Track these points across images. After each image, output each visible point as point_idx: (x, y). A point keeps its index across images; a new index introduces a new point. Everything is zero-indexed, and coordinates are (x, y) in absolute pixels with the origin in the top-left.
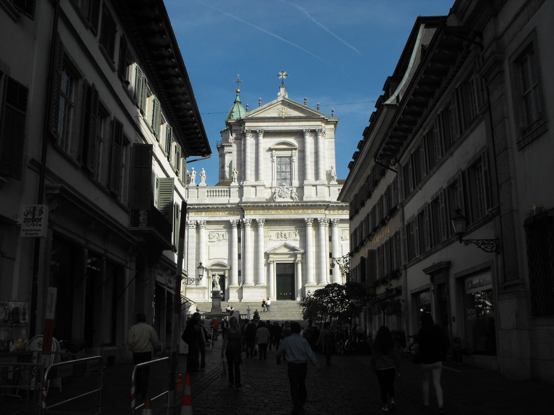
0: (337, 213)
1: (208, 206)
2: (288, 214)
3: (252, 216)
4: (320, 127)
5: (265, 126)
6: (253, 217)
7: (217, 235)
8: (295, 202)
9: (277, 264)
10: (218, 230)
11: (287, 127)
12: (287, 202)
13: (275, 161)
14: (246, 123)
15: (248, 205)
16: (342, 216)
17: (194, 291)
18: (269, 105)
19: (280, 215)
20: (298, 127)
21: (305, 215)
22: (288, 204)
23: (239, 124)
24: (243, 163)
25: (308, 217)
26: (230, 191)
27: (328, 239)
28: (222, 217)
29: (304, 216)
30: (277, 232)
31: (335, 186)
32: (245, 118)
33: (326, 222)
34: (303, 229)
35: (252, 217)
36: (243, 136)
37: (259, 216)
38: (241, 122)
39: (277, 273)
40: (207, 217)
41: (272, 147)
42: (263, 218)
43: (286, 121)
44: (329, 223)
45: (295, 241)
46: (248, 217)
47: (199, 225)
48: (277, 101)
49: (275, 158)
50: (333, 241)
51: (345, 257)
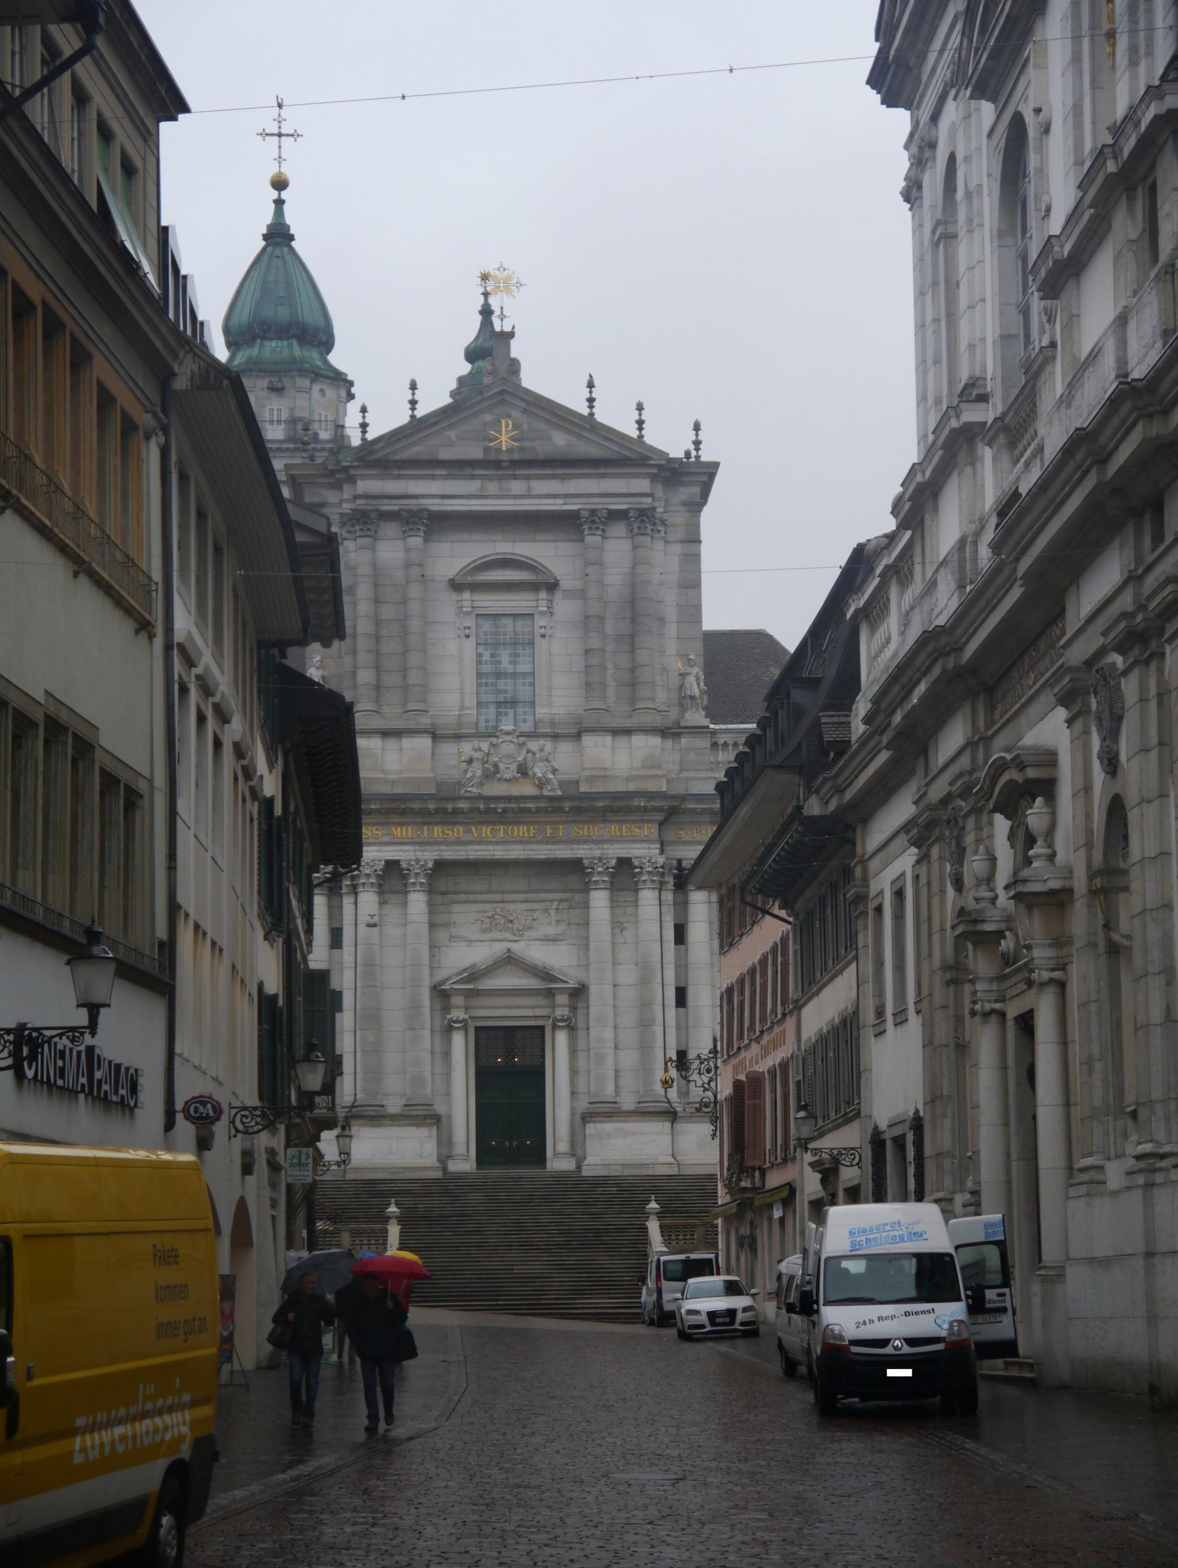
2: (521, 842)
3: (384, 848)
5: (433, 496)
6: (391, 853)
8: (550, 799)
9: (477, 1029)
11: (517, 502)
19: (490, 847)
20: (560, 501)
21: (585, 846)
23: (332, 481)
25: (597, 853)
27: (670, 934)
29: (583, 851)
31: (702, 732)
32: (355, 464)
36: (349, 532)
37: (411, 848)
38: (338, 476)
41: (458, 580)
43: (515, 477)
44: (675, 877)
45: (545, 943)
49: (470, 622)
51: (703, 1057)
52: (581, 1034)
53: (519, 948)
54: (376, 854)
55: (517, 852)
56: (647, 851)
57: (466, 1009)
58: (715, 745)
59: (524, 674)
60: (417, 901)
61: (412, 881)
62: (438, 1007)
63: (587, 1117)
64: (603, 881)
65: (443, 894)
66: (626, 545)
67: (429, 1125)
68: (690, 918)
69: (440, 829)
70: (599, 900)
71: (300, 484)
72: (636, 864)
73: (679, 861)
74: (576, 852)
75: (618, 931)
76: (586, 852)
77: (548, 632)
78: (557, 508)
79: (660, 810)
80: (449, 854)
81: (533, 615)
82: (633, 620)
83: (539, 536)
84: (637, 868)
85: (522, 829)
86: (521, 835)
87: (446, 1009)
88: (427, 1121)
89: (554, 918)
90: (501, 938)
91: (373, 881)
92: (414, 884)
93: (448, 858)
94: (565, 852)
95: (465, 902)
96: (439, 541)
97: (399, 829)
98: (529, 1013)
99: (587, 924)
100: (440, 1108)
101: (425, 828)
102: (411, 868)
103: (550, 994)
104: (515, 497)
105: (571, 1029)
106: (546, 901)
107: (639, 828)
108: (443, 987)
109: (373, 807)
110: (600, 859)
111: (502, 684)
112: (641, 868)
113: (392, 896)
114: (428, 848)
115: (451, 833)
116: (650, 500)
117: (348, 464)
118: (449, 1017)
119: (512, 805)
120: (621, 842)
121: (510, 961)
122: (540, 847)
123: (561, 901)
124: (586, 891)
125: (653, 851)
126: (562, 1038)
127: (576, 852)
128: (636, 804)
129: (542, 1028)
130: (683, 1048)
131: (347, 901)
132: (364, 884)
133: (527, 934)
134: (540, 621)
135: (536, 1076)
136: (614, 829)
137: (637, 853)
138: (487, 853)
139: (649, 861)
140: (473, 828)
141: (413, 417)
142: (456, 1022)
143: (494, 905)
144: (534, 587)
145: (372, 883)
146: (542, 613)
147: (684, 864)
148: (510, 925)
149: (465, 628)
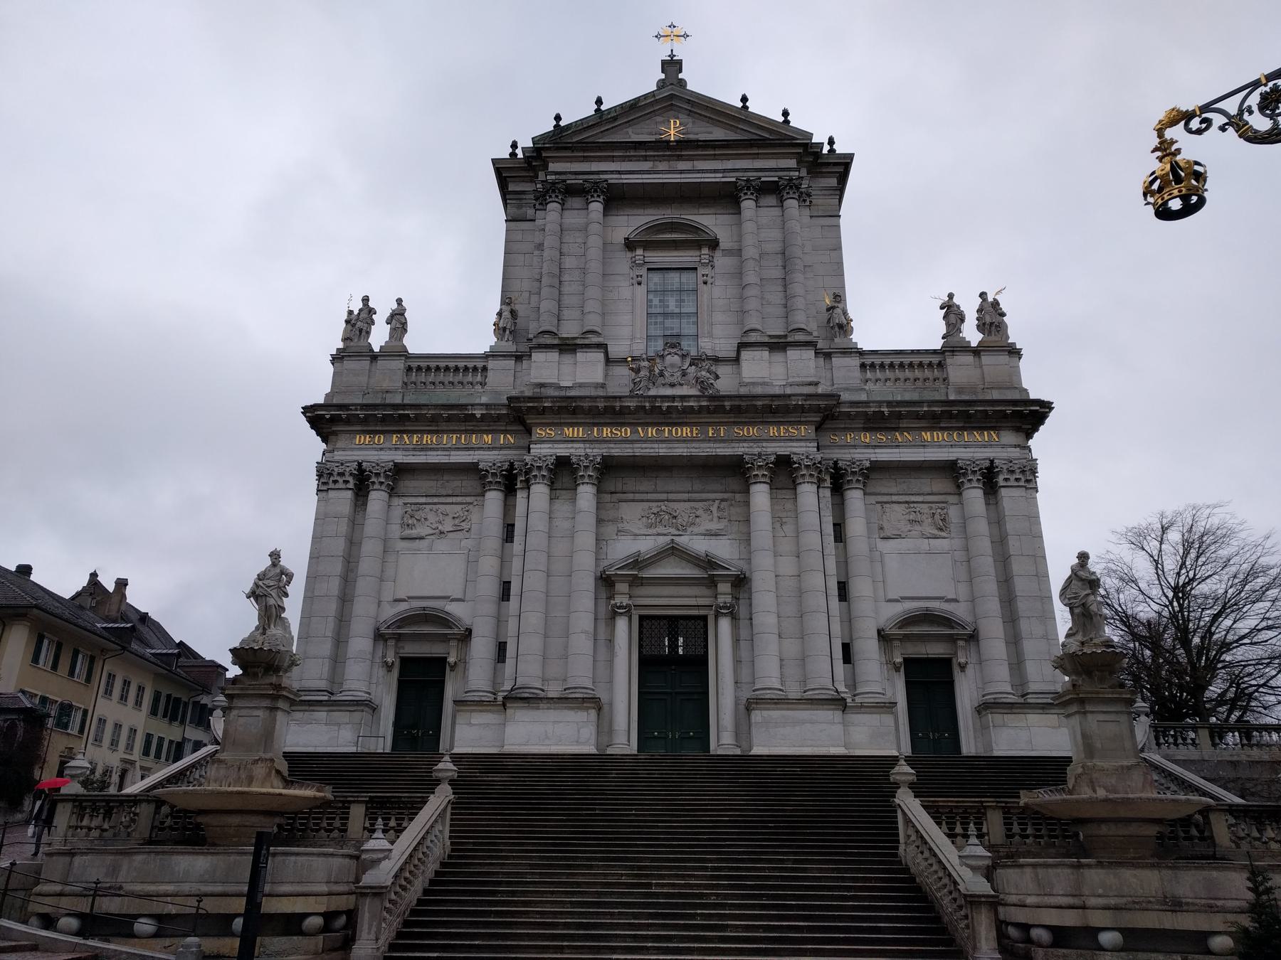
1: (402, 412)
2: (684, 441)
3: (556, 446)
4: (792, 173)
5: (612, 172)
6: (562, 450)
7: (432, 518)
8: (712, 398)
9: (642, 618)
10: (436, 500)
11: (683, 176)
12: (683, 398)
13: (644, 280)
14: (551, 165)
15: (544, 407)
16: (877, 451)
17: (322, 715)
19: (656, 446)
20: (721, 175)
21: (745, 445)
22: (685, 404)
25: (756, 451)
26: (485, 369)
27: (829, 529)
28: (452, 453)
30: (646, 505)
33: (821, 471)
34: (738, 496)
35: (558, 451)
37: (582, 445)
38: (534, 164)
39: (640, 652)
40: (399, 452)
43: (680, 158)
45: (706, 537)
46: (542, 451)
47: (369, 477)
48: (653, 99)
49: (643, 271)
50: (848, 540)
52: (743, 623)
53: (683, 540)
54: (548, 450)
55: (680, 450)
56: (804, 449)
57: (630, 597)
58: (863, 366)
59: (688, 315)
60: (586, 493)
62: (604, 596)
63: (750, 705)
64: (763, 475)
65: (612, 493)
66: (777, 211)
67: (587, 709)
68: (848, 515)
69: (609, 430)
70: (760, 495)
72: (795, 459)
73: (836, 463)
74: (736, 450)
75: (778, 525)
76: (747, 450)
77: (710, 281)
78: (718, 180)
79: (817, 409)
80: (616, 451)
81: (696, 269)
83: (702, 211)
84: (796, 463)
85: (685, 431)
86: (684, 435)
87: (611, 597)
88: (585, 705)
89: (715, 514)
90: (665, 532)
94: (726, 450)
95: (633, 501)
97: (571, 429)
98: (692, 602)
99: (748, 521)
100: (603, 695)
101: (595, 429)
102: (581, 463)
103: (712, 582)
104: (681, 172)
105: (734, 617)
106: (709, 500)
107: (797, 429)
109: (546, 405)
110: (760, 455)
111: (669, 323)
112: (799, 464)
113: (564, 492)
114: (597, 446)
115: (619, 434)
116: (797, 173)
118: (612, 602)
119: (676, 404)
120: (780, 441)
121: (672, 551)
122: (702, 445)
123: (722, 500)
124: (747, 491)
125: (810, 449)
126: (725, 625)
127: (736, 450)
128: (794, 403)
129: (705, 618)
130: (847, 641)
131: (521, 495)
132: (535, 476)
133: (689, 530)
134: (701, 271)
135: (698, 664)
136: (773, 431)
137: (795, 450)
138: (652, 451)
139: (807, 457)
140: (640, 429)
141: (598, 110)
142: (620, 607)
143: (659, 504)
144: (697, 245)
145: (544, 476)
146: (703, 264)
147: (840, 464)
148: (674, 521)
149: (637, 276)
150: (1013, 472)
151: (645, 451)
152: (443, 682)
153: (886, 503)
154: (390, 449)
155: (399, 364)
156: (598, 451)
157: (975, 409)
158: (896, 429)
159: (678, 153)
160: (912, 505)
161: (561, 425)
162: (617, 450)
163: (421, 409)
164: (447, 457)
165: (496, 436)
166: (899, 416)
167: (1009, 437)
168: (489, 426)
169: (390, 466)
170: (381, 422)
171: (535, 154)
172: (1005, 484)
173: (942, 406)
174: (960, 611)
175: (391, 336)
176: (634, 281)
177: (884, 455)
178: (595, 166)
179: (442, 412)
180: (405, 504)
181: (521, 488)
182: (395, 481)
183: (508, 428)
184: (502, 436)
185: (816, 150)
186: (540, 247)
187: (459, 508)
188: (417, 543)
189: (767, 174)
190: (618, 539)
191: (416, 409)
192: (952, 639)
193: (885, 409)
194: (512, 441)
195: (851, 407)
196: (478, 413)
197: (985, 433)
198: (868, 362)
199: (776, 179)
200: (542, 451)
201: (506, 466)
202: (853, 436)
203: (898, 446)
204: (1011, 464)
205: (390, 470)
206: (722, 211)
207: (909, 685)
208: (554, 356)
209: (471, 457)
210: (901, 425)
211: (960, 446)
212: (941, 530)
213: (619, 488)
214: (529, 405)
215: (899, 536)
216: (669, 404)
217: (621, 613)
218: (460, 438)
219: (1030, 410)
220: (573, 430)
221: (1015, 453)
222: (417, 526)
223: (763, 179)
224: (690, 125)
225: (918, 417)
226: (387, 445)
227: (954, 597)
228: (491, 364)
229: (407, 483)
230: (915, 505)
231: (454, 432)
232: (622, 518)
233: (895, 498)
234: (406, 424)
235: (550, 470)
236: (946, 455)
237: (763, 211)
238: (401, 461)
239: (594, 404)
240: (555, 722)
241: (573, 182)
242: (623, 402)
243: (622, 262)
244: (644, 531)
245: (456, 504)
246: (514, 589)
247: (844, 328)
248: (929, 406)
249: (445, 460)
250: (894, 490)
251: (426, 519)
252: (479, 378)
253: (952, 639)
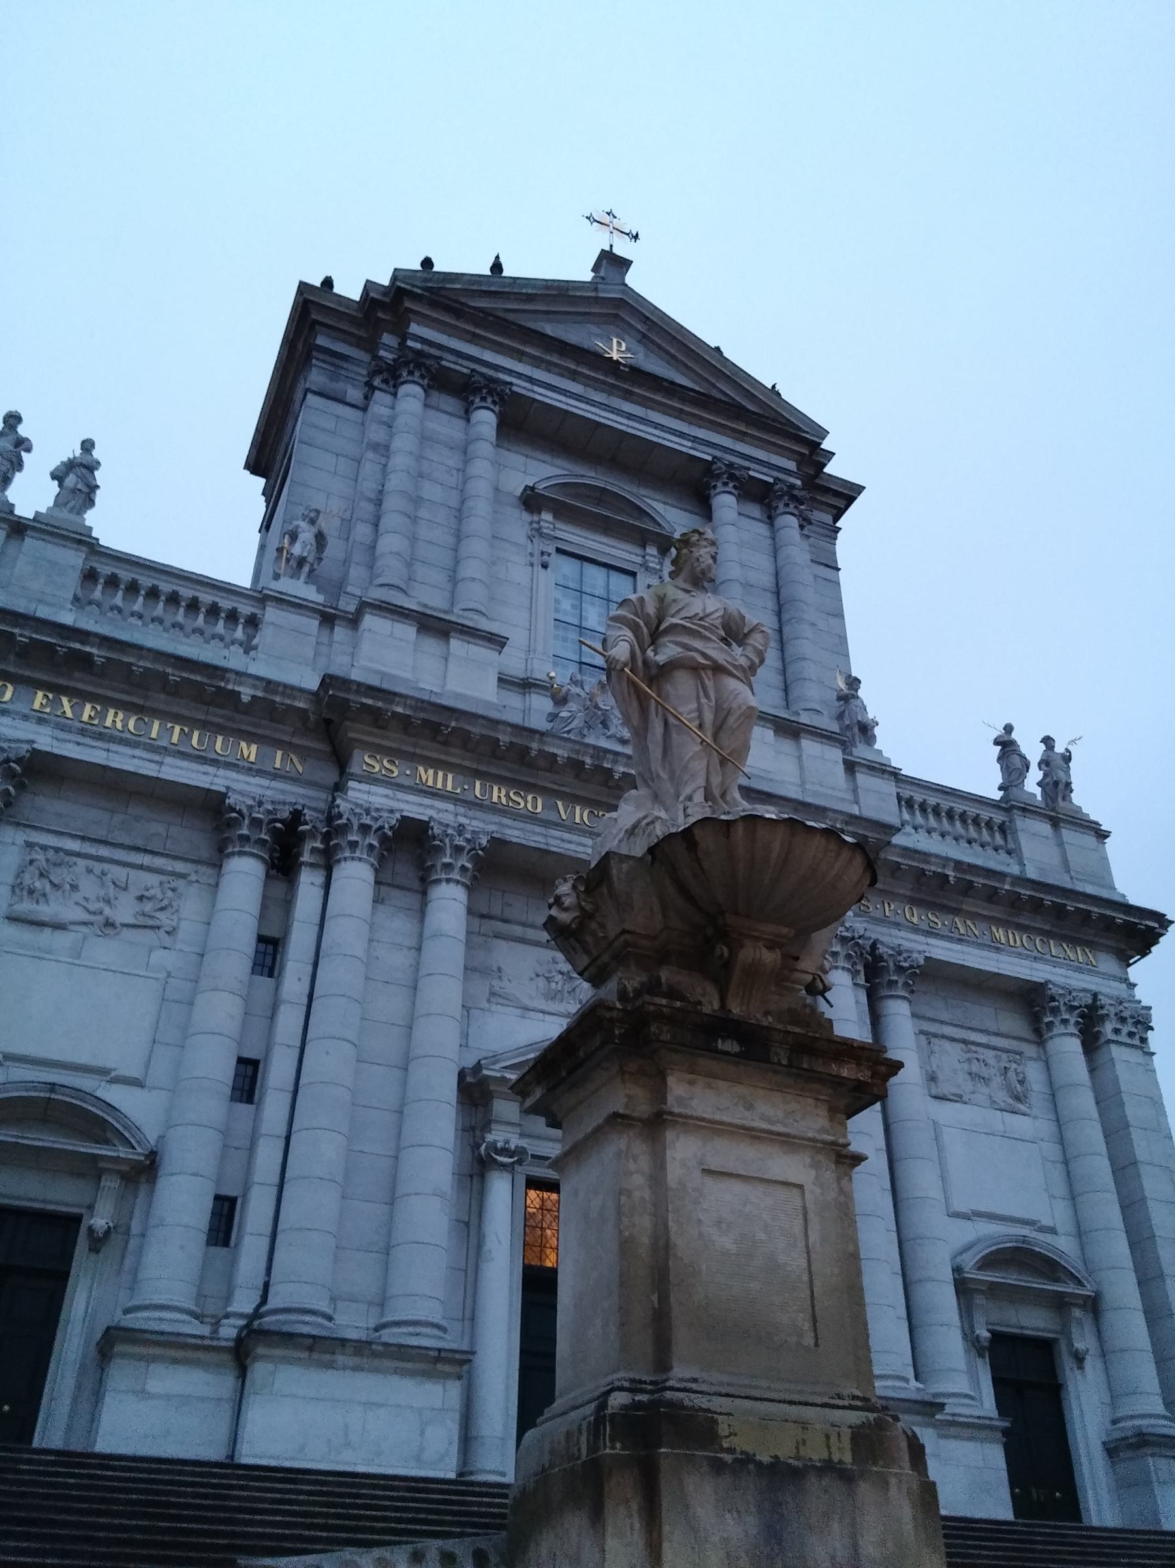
0: (900, 919)
1: (77, 646)
3: (400, 795)
4: (792, 480)
5: (520, 376)
6: (415, 807)
7: (89, 887)
10: (104, 852)
11: (631, 423)
15: (394, 713)
16: (932, 941)
18: (554, 292)
20: (689, 444)
24: (367, 508)
26: (253, 622)
28: (168, 760)
32: (415, 290)
36: (385, 381)
37: (451, 807)
38: (380, 315)
40: (46, 730)
42: (477, 825)
43: (628, 396)
48: (593, 294)
49: (551, 549)
61: (447, 860)
66: (762, 529)
69: (503, 792)
71: (316, 322)
80: (515, 833)
81: (633, 574)
82: (779, 613)
91: (375, 843)
92: (448, 867)
93: (514, 840)
96: (509, 450)
97: (431, 772)
102: (447, 841)
104: (630, 416)
108: (485, 1072)
113: (395, 893)
114: (479, 814)
117: (408, 287)
132: (353, 845)
138: (580, 849)
140: (560, 804)
145: (371, 846)
147: (882, 949)
149: (543, 553)
150: (1123, 1020)
151: (567, 846)
152: (65, 1276)
153: (935, 1036)
154: (25, 718)
155: (75, 559)
156: (481, 825)
157: (1075, 905)
158: (956, 911)
159: (626, 387)
160: (974, 1048)
161: (413, 758)
162: (516, 833)
163: (123, 652)
164: (156, 767)
165: (268, 750)
166: (967, 889)
167: (1107, 963)
168: (256, 725)
169: (23, 753)
170: (18, 655)
171: (387, 300)
172: (1114, 1037)
173: (1033, 889)
174: (1064, 1245)
175: (57, 503)
176: (537, 560)
177: (943, 951)
178: (488, 356)
179: (169, 670)
180: (30, 845)
181: (312, 865)
182: (21, 787)
183: (296, 741)
184: (279, 753)
185: (822, 460)
186: (384, 450)
187: (153, 879)
188: (46, 936)
189: (757, 467)
190: (489, 1010)
191: (110, 649)
192: (1060, 1304)
193: (951, 873)
194: (300, 769)
195: (902, 856)
196: (246, 693)
197: (1078, 948)
198: (906, 794)
199: (771, 480)
200: (372, 799)
201: (285, 814)
202: (892, 908)
203: (960, 941)
204: (1121, 1008)
205: (19, 761)
206: (675, 503)
207: (998, 1383)
208: (408, 631)
209: (208, 779)
210: (964, 907)
211: (1047, 962)
212: (1018, 1099)
213: (496, 910)
214: (364, 700)
215: (958, 1099)
216: (626, 770)
217: (504, 1166)
218: (189, 737)
219: (1146, 926)
220: (436, 774)
221: (1119, 989)
222: (51, 897)
223: (751, 473)
224: (641, 356)
225: (992, 896)
226: (19, 707)
227: (1052, 1225)
228: (271, 614)
229: (41, 801)
230: (978, 1049)
231: (177, 718)
232: (499, 970)
233: (948, 1030)
234: (77, 674)
235: (384, 839)
236: (1028, 972)
237: (745, 522)
238: (48, 749)
239: (492, 734)
240: (369, 1405)
241: (452, 366)
242: (544, 743)
243: (518, 523)
244: (542, 1004)
245: (149, 869)
246: (278, 1072)
247: (866, 730)
248: (1012, 884)
249: (149, 770)
250: (945, 1016)
251: (74, 887)
252: (239, 633)
253: (1060, 1304)
